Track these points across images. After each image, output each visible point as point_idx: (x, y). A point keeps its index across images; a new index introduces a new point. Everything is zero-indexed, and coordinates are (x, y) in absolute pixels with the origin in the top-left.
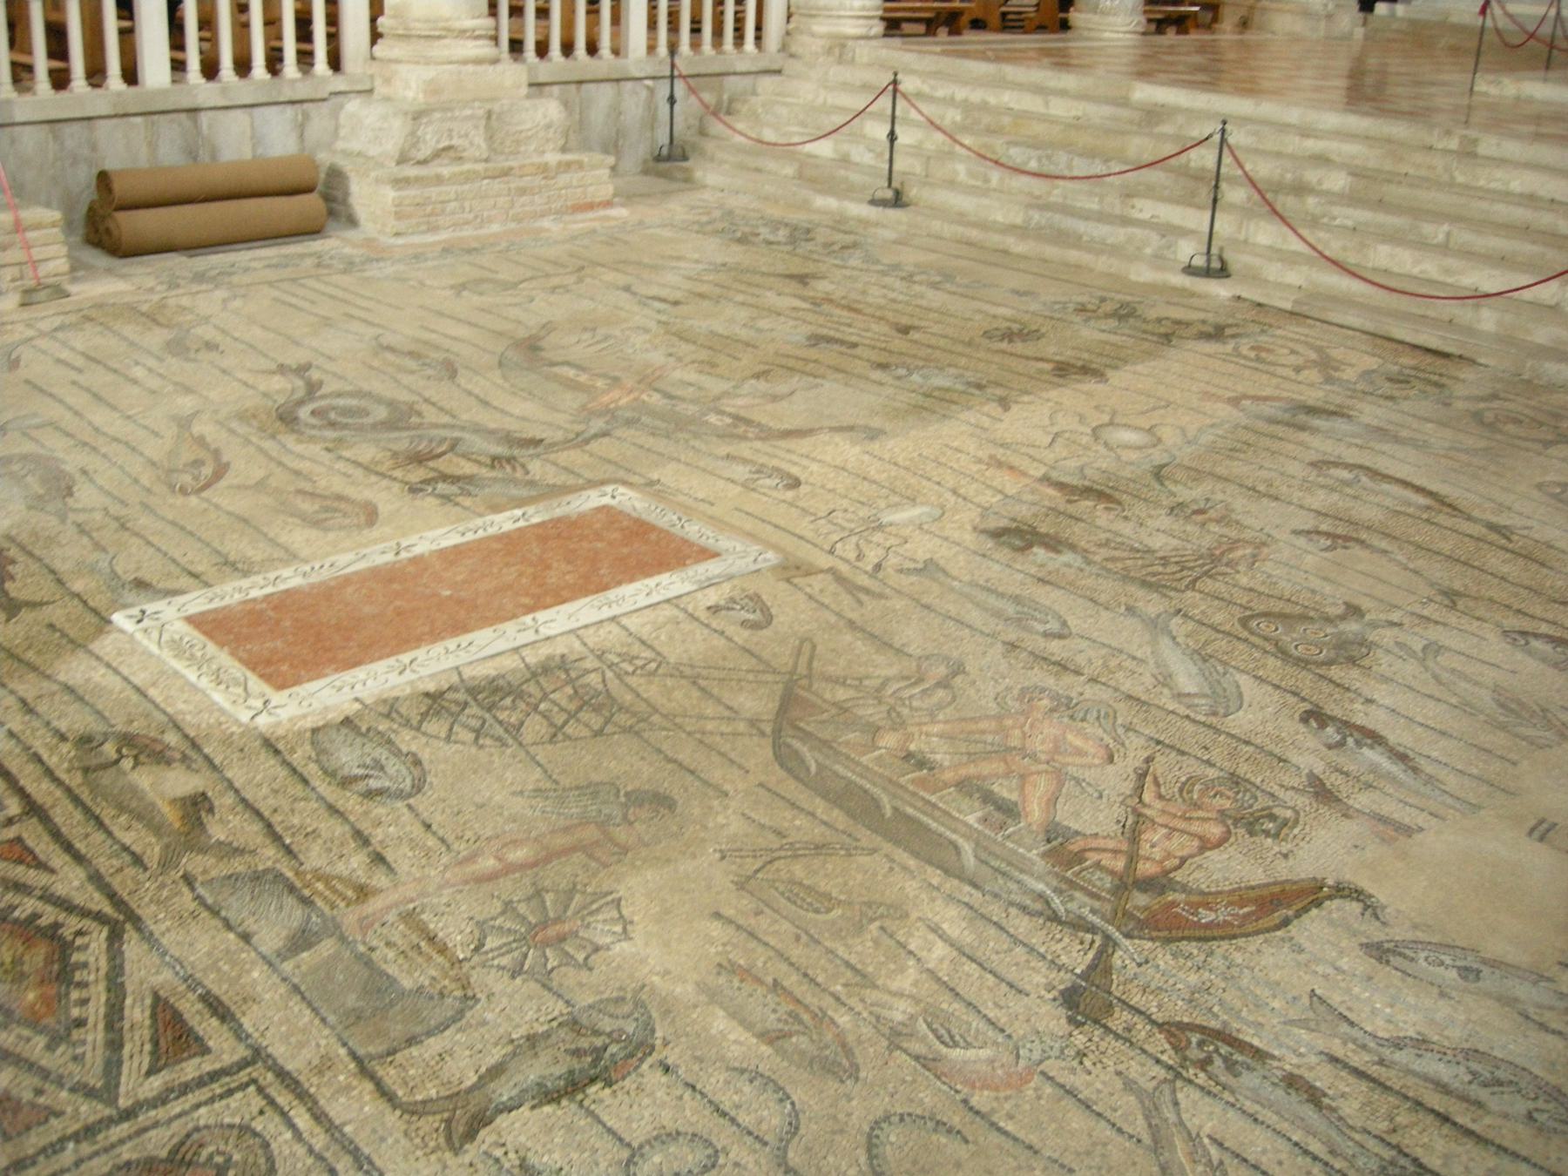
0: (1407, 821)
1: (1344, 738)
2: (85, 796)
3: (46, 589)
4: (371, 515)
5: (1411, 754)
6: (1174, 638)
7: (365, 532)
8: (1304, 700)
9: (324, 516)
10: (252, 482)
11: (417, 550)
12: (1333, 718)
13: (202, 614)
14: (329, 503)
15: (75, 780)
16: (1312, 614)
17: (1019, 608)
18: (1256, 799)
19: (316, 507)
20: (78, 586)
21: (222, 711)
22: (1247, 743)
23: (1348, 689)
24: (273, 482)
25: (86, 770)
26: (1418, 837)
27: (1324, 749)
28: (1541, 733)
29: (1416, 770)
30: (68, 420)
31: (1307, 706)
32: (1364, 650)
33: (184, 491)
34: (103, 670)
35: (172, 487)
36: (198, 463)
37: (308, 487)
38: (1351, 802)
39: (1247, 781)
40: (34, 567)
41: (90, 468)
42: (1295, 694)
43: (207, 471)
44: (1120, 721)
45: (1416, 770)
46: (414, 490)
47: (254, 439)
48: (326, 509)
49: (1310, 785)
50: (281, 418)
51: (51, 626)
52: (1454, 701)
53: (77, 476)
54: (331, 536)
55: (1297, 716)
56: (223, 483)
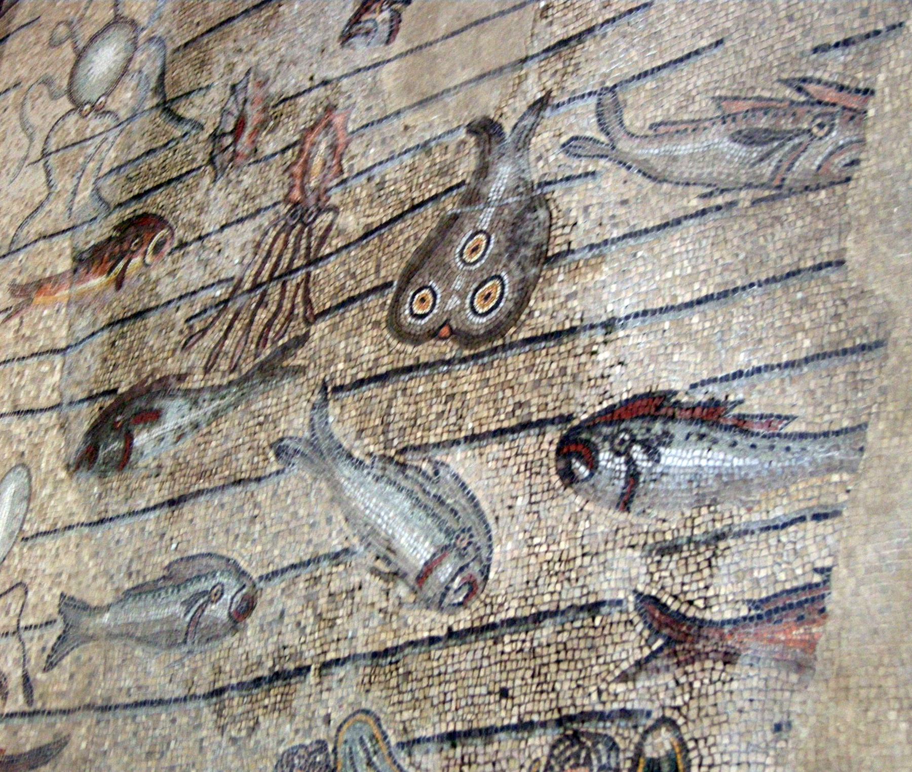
0: (802, 576)
1: (630, 462)
5: (717, 391)
6: (350, 456)
8: (541, 423)
12: (592, 424)
16: (450, 206)
17: (185, 594)
18: (613, 747)
22: (538, 618)
23: (573, 330)
26: (833, 601)
27: (622, 517)
28: (827, 146)
29: (741, 425)
31: (553, 434)
32: (542, 214)
38: (713, 614)
39: (586, 716)
42: (525, 426)
44: (393, 740)
45: (741, 425)
49: (657, 633)
52: (695, 204)
55: (555, 479)
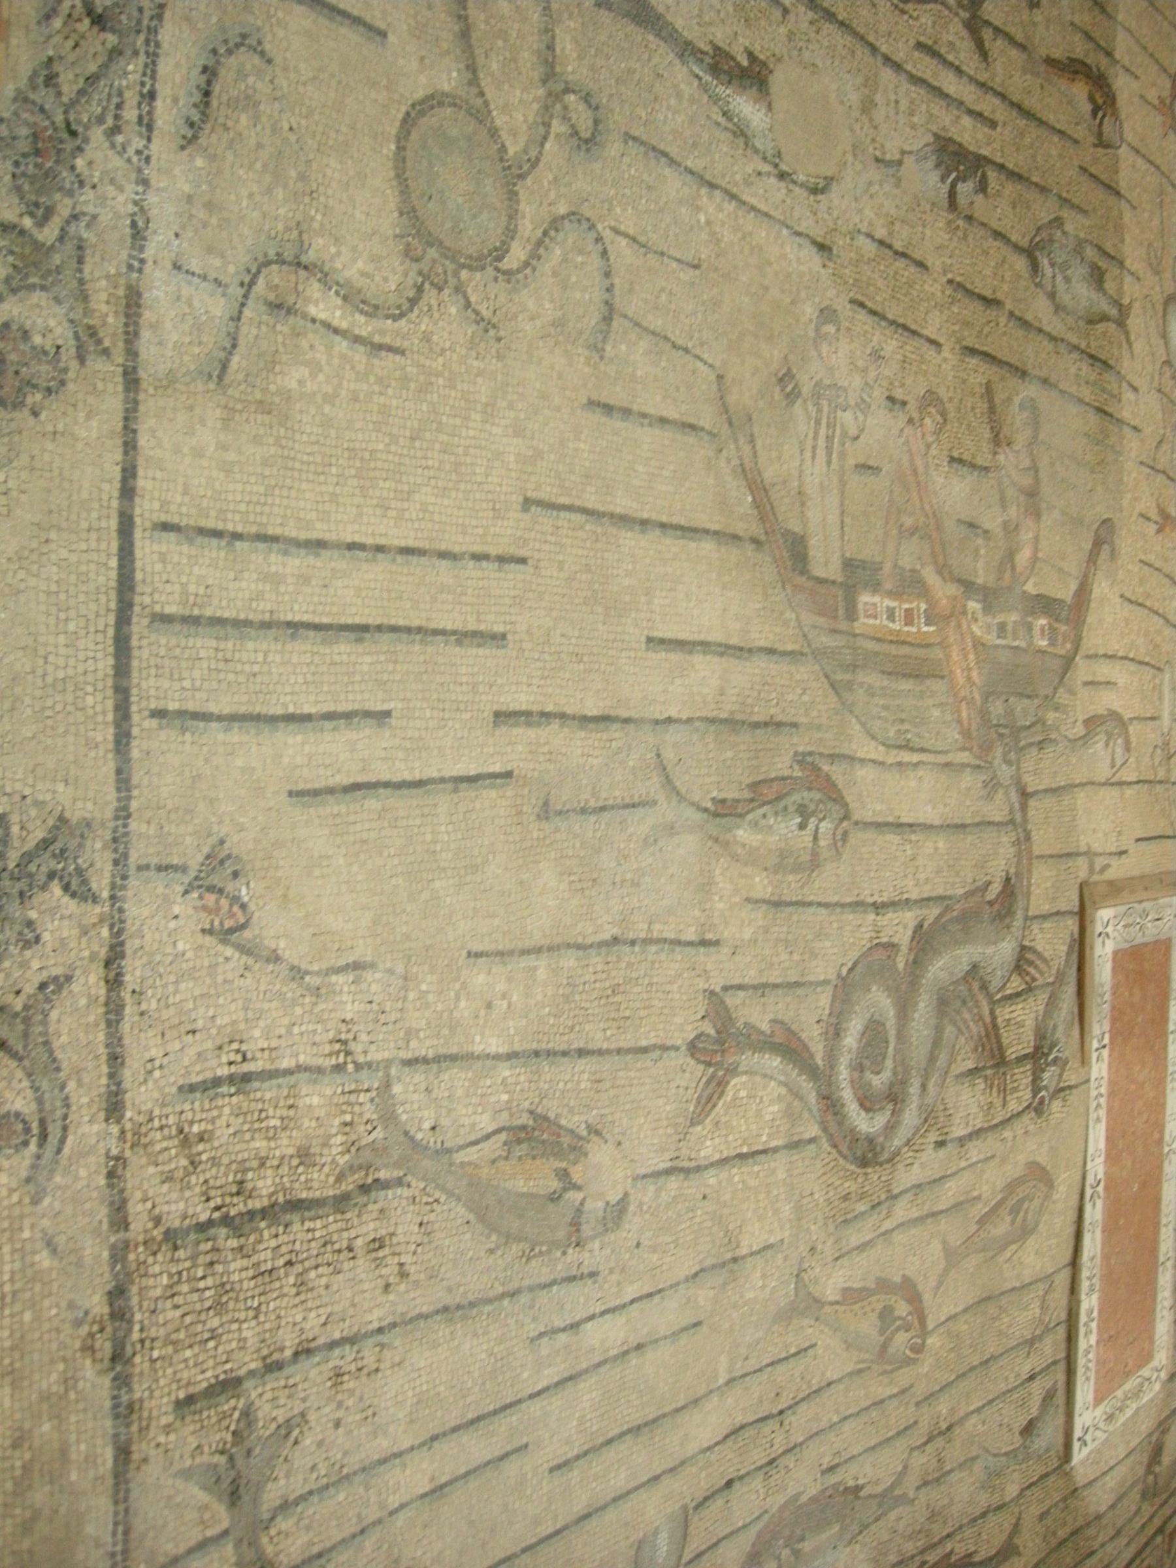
2: (1164, 1496)
3: (1005, 1521)
4: (1040, 1175)
7: (1056, 1197)
9: (1019, 1219)
10: (942, 1264)
11: (1100, 1175)
13: (1096, 1391)
14: (1010, 1203)
15: (1158, 1501)
19: (1008, 1219)
20: (1012, 1490)
21: (1152, 1400)
24: (955, 1240)
25: (1155, 1495)
30: (685, 1487)
33: (918, 1349)
34: (1107, 1478)
35: (908, 1362)
36: (886, 1314)
37: (979, 1210)
40: (968, 1532)
41: (826, 1462)
43: (902, 1309)
46: (1038, 1109)
47: (888, 1225)
48: (1015, 1211)
50: (864, 1163)
51: (1042, 1516)
53: (833, 1479)
54: (1042, 1227)
56: (927, 1297)
